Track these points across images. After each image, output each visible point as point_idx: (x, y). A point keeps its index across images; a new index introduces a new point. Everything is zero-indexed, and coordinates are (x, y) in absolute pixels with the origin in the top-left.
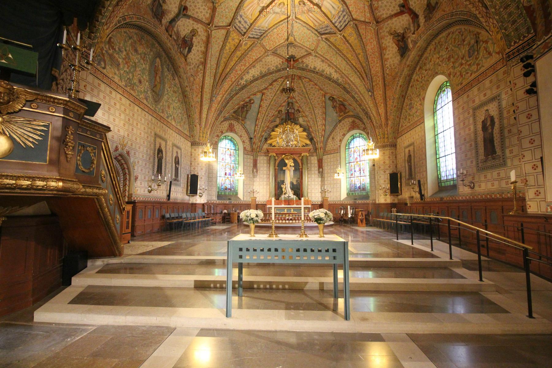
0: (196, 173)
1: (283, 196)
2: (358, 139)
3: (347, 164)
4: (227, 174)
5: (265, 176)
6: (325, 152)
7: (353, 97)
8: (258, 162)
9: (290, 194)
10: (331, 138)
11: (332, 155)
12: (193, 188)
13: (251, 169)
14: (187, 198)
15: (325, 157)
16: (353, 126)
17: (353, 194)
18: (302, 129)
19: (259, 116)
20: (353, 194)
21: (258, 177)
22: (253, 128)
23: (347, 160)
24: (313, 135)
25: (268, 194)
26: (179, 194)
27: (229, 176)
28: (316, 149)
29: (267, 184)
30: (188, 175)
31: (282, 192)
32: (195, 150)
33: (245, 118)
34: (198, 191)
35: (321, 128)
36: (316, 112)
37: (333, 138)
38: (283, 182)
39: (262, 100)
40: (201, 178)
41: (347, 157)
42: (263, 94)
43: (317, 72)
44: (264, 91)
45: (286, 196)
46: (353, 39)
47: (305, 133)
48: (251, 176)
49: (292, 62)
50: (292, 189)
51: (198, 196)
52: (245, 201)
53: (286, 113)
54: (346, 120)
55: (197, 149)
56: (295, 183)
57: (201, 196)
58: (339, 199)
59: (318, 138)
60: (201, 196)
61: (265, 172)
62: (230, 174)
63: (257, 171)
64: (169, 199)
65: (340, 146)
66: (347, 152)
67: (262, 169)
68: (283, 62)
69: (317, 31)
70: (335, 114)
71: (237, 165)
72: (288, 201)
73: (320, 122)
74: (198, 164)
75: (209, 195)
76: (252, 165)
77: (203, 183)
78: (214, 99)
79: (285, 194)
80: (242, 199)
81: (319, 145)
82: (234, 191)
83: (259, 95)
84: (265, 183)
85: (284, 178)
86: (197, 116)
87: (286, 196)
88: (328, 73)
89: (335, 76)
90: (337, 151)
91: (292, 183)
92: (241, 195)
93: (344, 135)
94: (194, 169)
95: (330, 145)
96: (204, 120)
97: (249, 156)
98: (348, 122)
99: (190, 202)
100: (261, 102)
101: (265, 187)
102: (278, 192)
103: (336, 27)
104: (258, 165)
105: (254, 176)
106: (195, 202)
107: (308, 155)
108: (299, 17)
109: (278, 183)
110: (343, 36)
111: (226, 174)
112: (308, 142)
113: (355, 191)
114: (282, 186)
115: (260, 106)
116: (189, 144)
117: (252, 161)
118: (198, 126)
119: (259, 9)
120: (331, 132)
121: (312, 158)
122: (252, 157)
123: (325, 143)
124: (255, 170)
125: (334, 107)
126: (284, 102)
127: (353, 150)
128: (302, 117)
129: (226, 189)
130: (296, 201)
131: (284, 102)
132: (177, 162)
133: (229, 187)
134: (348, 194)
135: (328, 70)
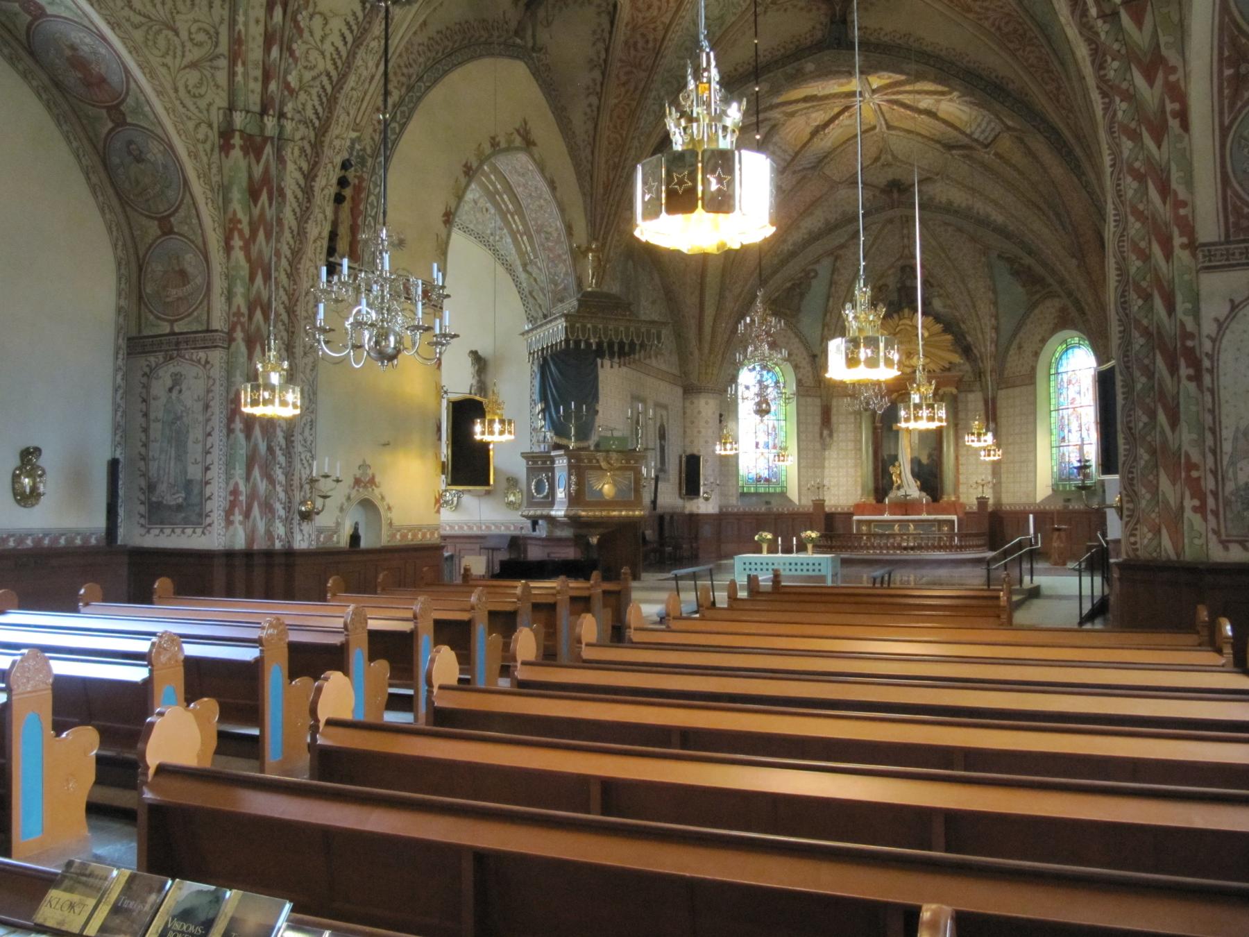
0: (696, 452)
1: (893, 494)
2: (1076, 350)
3: (1053, 414)
4: (761, 445)
5: (851, 445)
6: (1004, 382)
7: (1044, 264)
8: (834, 411)
9: (911, 489)
10: (1014, 346)
11: (1017, 390)
12: (691, 485)
13: (817, 429)
14: (679, 502)
15: (1002, 393)
16: (1064, 322)
17: (1064, 486)
18: (939, 327)
19: (831, 303)
20: (1064, 486)
21: (834, 447)
22: (819, 332)
23: (1053, 401)
24: (969, 339)
25: (859, 489)
26: (669, 497)
27: (766, 451)
28: (979, 374)
29: (856, 466)
30: (681, 457)
31: (892, 483)
32: (692, 403)
33: (799, 310)
34: (702, 489)
35: (988, 322)
36: (971, 285)
37: (1020, 347)
38: (894, 459)
39: (834, 270)
40: (706, 461)
41: (1052, 396)
42: (837, 258)
43: (956, 212)
44: (841, 252)
45: (901, 492)
46: (1018, 157)
47: (949, 337)
48: (818, 446)
49: (895, 195)
50: (915, 475)
51: (701, 500)
52: (804, 506)
53: (899, 290)
54: (1048, 303)
55: (695, 401)
56: (925, 460)
57: (707, 499)
58: (1031, 500)
59: (986, 347)
60: (707, 499)
61: (851, 436)
62: (767, 446)
63: (831, 435)
64: (655, 508)
65: (1034, 369)
66: (1052, 384)
67: (842, 427)
68: (874, 196)
69: (938, 142)
70: (1020, 289)
71: (783, 423)
72: (906, 506)
73: (984, 308)
74: (699, 432)
75: (723, 495)
76: (818, 420)
77: (710, 472)
78: (727, 294)
79: (899, 488)
80: (797, 502)
81: (989, 365)
82: (777, 483)
83: (827, 262)
84: (851, 462)
85: (897, 449)
86: (692, 335)
87: (901, 492)
88: (981, 211)
89: (998, 218)
90: (1030, 379)
91: (915, 462)
92: (793, 494)
93: (1044, 341)
94: (692, 442)
95: (1014, 364)
96: (708, 338)
97: (809, 399)
98: (1050, 309)
99: (687, 511)
100: (833, 273)
101: (852, 471)
102: (882, 485)
103: (976, 140)
104: (834, 419)
105: (825, 447)
106: (695, 510)
107: (954, 391)
108: (896, 124)
109: (883, 460)
110: (996, 154)
111: (757, 444)
112: (956, 359)
113: (1070, 480)
114: (891, 469)
115: (832, 283)
116: (680, 391)
117: (818, 411)
118: (696, 352)
119: (809, 130)
120: (1014, 335)
121: (971, 396)
122: (818, 401)
123: (1001, 358)
124: (826, 432)
125: (1016, 273)
126: (889, 268)
127: (1065, 377)
128: (940, 296)
129: (759, 479)
130: (928, 504)
131: (889, 268)
132: (662, 436)
133: (765, 474)
134: (1055, 490)
135: (980, 206)
